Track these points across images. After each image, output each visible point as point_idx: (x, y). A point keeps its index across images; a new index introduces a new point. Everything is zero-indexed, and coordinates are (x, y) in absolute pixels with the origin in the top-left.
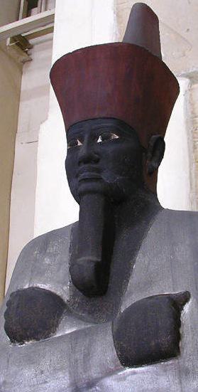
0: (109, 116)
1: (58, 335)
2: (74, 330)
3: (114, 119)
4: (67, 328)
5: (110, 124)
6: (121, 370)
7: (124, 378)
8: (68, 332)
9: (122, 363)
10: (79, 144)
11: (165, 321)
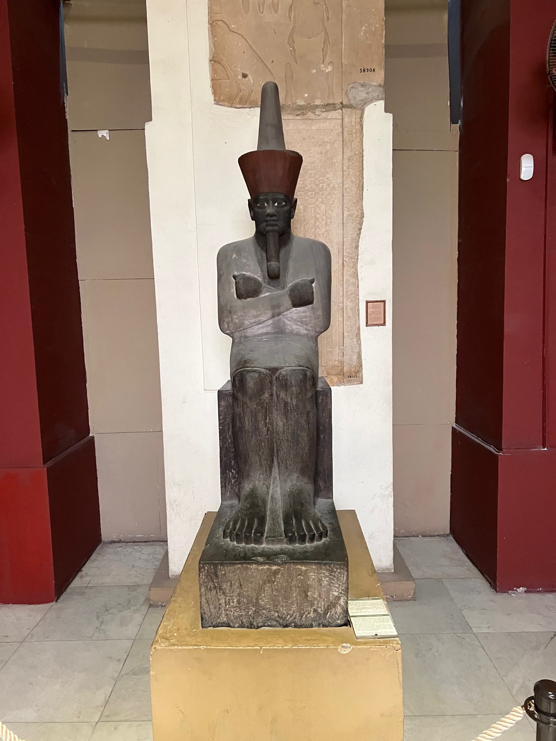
8: (267, 294)
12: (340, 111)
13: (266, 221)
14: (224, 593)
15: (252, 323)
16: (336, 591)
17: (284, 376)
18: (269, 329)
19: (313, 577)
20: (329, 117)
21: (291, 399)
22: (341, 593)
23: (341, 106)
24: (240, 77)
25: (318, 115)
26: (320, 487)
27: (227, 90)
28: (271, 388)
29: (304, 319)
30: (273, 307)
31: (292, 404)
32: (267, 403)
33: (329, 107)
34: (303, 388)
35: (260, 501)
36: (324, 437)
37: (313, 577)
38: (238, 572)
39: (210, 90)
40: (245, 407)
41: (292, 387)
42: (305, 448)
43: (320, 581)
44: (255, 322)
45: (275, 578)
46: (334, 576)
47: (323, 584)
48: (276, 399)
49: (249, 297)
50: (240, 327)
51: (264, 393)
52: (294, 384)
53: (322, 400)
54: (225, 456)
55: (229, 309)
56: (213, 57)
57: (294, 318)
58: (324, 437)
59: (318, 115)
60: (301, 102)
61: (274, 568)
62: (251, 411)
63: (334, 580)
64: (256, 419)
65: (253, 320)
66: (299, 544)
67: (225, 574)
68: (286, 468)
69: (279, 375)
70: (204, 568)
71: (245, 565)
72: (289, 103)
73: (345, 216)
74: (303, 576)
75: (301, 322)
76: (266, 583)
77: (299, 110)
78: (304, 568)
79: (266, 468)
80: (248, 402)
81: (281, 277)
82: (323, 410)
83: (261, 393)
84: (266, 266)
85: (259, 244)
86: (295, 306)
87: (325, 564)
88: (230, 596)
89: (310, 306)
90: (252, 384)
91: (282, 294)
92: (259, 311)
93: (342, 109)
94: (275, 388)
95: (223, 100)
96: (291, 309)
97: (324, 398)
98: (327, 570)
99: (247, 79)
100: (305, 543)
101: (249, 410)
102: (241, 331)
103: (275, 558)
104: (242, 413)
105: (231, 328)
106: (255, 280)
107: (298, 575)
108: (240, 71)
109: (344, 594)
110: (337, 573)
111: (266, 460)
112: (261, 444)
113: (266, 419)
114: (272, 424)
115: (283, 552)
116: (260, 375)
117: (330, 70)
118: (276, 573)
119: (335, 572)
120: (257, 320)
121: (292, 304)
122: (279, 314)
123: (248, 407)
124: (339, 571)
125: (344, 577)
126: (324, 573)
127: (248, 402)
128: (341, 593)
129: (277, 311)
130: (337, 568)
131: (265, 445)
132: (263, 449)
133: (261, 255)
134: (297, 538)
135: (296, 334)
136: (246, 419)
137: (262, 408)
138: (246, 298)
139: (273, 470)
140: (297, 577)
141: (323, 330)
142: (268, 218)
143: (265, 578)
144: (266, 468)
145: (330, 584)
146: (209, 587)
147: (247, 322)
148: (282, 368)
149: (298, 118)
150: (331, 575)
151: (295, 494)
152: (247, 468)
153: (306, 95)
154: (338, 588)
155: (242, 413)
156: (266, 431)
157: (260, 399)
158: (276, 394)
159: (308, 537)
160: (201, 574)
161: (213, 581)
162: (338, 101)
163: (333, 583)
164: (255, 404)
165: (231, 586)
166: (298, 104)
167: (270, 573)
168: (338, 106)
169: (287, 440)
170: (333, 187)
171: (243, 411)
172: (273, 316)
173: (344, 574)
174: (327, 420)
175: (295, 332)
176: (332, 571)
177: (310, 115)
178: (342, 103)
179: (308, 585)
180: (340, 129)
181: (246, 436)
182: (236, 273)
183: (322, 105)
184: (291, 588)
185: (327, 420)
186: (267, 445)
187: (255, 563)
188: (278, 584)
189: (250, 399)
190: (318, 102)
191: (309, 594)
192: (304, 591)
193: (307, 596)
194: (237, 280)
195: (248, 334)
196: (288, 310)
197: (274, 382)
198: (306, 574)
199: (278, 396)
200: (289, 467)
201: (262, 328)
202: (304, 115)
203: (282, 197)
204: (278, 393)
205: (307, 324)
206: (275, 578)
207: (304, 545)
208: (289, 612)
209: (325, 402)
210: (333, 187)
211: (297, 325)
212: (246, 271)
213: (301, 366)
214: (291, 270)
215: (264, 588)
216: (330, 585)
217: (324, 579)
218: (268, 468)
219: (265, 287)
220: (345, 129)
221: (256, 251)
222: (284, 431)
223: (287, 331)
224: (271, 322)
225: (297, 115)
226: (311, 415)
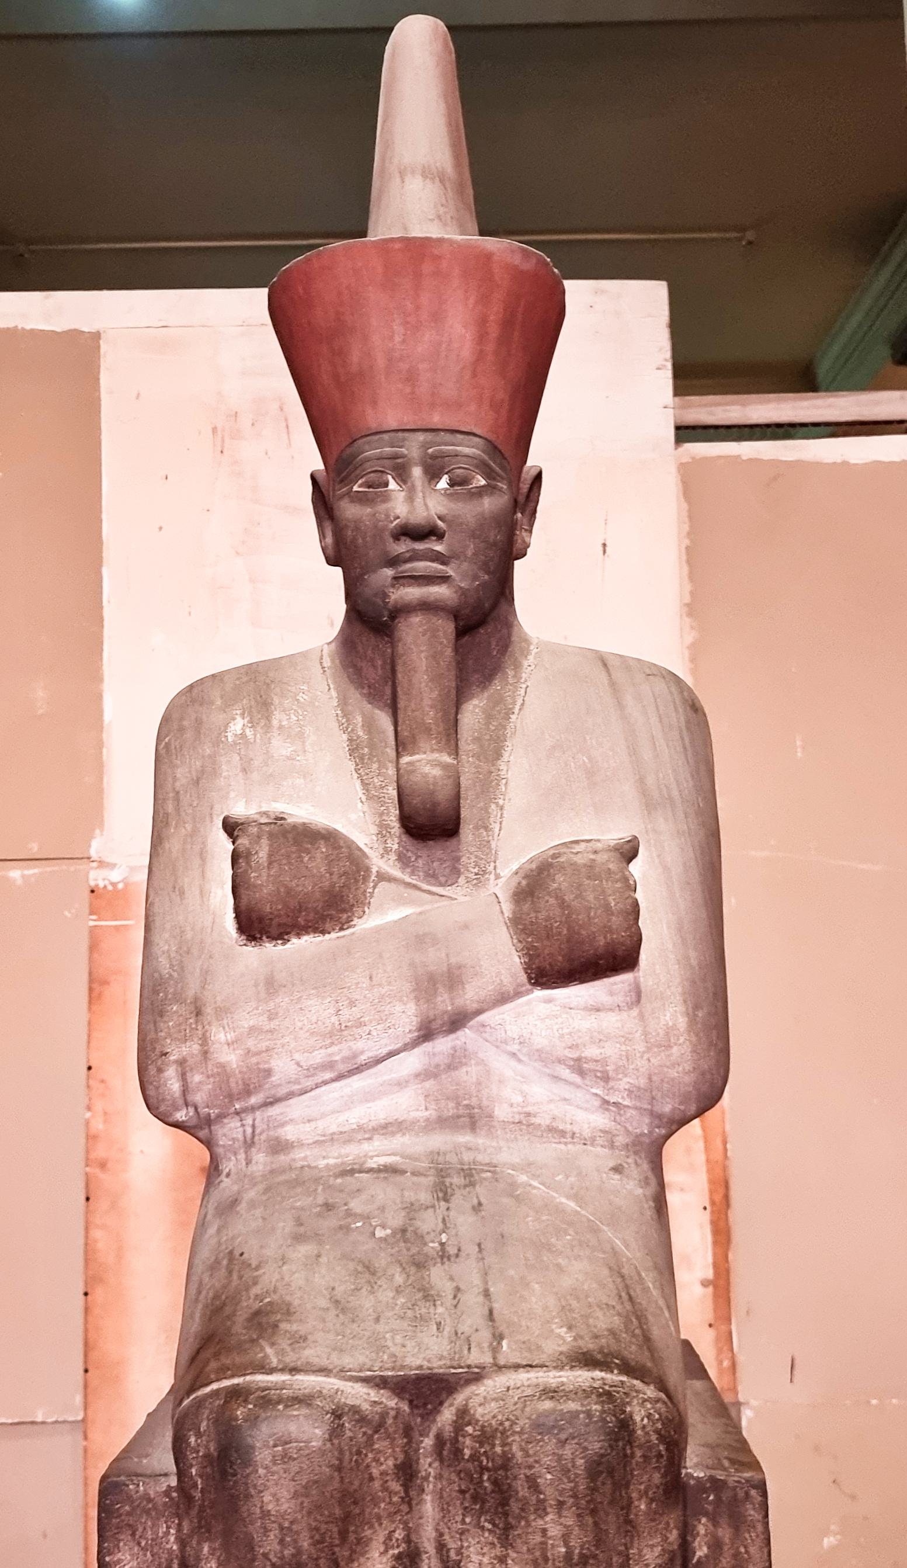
8: (396, 914)
9: (530, 979)
15: (311, 1071)
17: (485, 1436)
18: (408, 1104)
28: (409, 1501)
30: (427, 985)
41: (541, 1509)
44: (329, 1065)
49: (302, 930)
50: (248, 1092)
52: (550, 1494)
55: (190, 994)
57: (540, 1042)
65: (319, 1057)
81: (467, 832)
84: (391, 771)
90: (285, 1494)
91: (475, 918)
92: (352, 1004)
94: (429, 1507)
102: (253, 1109)
105: (199, 1098)
116: (335, 1432)
120: (339, 1052)
121: (527, 968)
122: (457, 1022)
129: (445, 1003)
133: (370, 725)
135: (551, 1129)
138: (281, 935)
141: (693, 1109)
148: (476, 1376)
158: (441, 1547)
172: (426, 1033)
175: (543, 1120)
182: (240, 809)
194: (243, 841)
195: (289, 1133)
196: (503, 998)
197: (427, 1465)
203: (469, 449)
219: (382, 877)
221: (343, 702)
223: (501, 1112)
224: (413, 1061)
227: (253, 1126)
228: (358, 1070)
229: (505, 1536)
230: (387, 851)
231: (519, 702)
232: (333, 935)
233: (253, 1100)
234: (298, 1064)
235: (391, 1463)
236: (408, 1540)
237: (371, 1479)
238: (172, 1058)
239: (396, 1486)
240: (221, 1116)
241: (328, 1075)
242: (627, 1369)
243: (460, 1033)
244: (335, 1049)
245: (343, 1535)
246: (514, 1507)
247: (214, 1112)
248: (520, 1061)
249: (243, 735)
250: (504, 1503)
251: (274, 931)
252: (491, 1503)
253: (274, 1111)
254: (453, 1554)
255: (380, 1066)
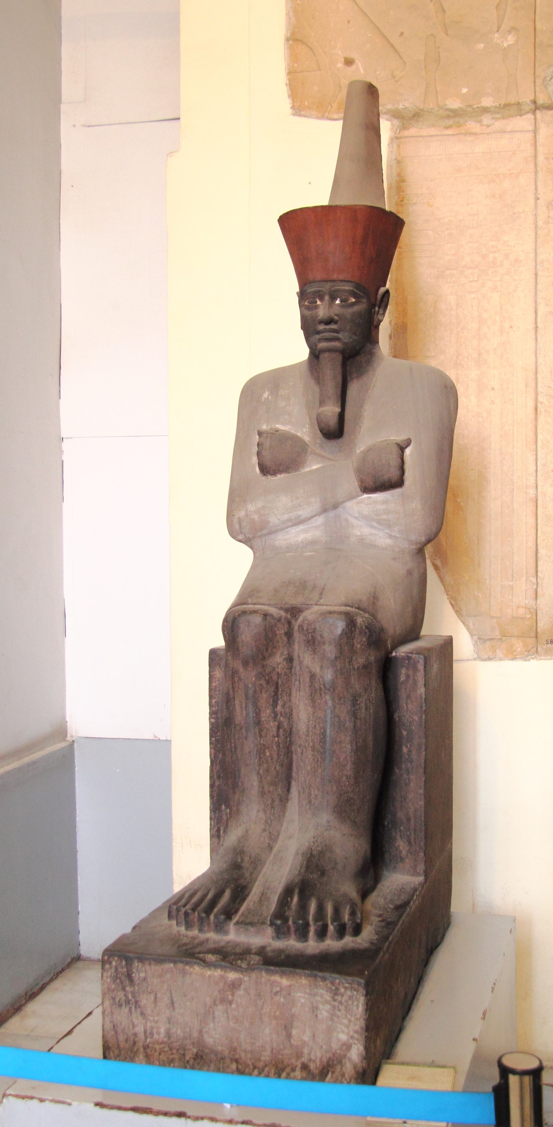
0: (347, 279)
1: (307, 469)
2: (319, 466)
3: (351, 282)
4: (313, 466)
5: (348, 287)
6: (361, 496)
7: (362, 502)
8: (314, 467)
9: (361, 490)
10: (319, 303)
11: (394, 462)
12: (530, 116)
13: (318, 333)
14: (142, 1014)
16: (343, 1032)
19: (303, 1000)
20: (509, 129)
21: (321, 667)
22: (352, 1037)
23: (532, 107)
24: (340, 65)
25: (488, 126)
26: (401, 852)
27: (316, 88)
29: (384, 517)
31: (322, 677)
32: (278, 674)
33: (509, 109)
34: (346, 649)
35: (246, 859)
36: (410, 751)
37: (303, 1000)
38: (168, 976)
39: (283, 91)
40: (236, 679)
41: (324, 643)
42: (345, 766)
43: (314, 1009)
44: (290, 520)
45: (233, 995)
46: (341, 1003)
47: (320, 1017)
48: (298, 668)
50: (262, 529)
51: (272, 655)
53: (408, 676)
54: (219, 777)
56: (293, 33)
58: (410, 751)
59: (488, 126)
60: (454, 104)
61: (232, 976)
62: (246, 687)
63: (339, 1010)
64: (255, 704)
65: (286, 517)
66: (294, 940)
67: (145, 979)
68: (310, 802)
69: (303, 621)
70: (110, 963)
71: (180, 966)
72: (431, 106)
73: (539, 314)
74: (285, 997)
75: (379, 522)
76: (218, 1002)
77: (448, 117)
78: (285, 982)
79: (273, 801)
80: (241, 669)
82: (409, 697)
83: (266, 654)
85: (312, 373)
86: (367, 489)
87: (324, 979)
88: (154, 1021)
89: (397, 491)
92: (297, 498)
93: (534, 112)
95: (309, 108)
96: (358, 496)
97: (411, 672)
98: (329, 990)
99: (353, 67)
100: (306, 940)
101: (242, 686)
103: (239, 959)
104: (231, 692)
105: (245, 531)
106: (295, 439)
107: (276, 993)
108: (340, 55)
109: (357, 1040)
110: (345, 998)
111: (274, 784)
112: (264, 752)
113: (275, 704)
114: (289, 716)
115: (261, 951)
117: (511, 43)
118: (234, 986)
119: (342, 996)
122: (335, 507)
123: (240, 679)
124: (349, 993)
125: (358, 1007)
126: (322, 996)
127: (241, 669)
128: (352, 1037)
130: (346, 988)
131: (271, 756)
132: (267, 762)
134: (292, 929)
136: (237, 702)
137: (268, 682)
138: (274, 473)
139: (289, 805)
140: (272, 998)
142: (321, 327)
143: (216, 993)
144: (273, 801)
145: (332, 1017)
146: (117, 1000)
147: (274, 520)
148: (308, 606)
149: (449, 132)
150: (335, 1000)
151: (315, 853)
152: (236, 797)
153: (465, 91)
154: (347, 1027)
155: (231, 692)
156: (275, 730)
157: (263, 666)
159: (312, 929)
160: (105, 974)
161: (124, 989)
162: (527, 98)
163: (338, 1017)
164: (254, 673)
165: (155, 1001)
166: (449, 106)
167: (225, 983)
168: (527, 108)
169: (313, 749)
170: (517, 260)
171: (233, 688)
172: (324, 510)
173: (358, 1000)
174: (416, 718)
176: (336, 993)
177: (472, 125)
178: (534, 102)
179: (293, 1015)
180: (530, 151)
181: (237, 736)
182: (264, 427)
183: (496, 107)
184: (261, 1018)
185: (416, 718)
186: (275, 756)
187: (198, 964)
188: (238, 1005)
189: (245, 664)
190: (487, 102)
191: (294, 1032)
192: (286, 1027)
193: (289, 1036)
196: (351, 498)
197: (296, 635)
198: (289, 994)
199: (301, 662)
200: (313, 801)
201: (306, 531)
202: (459, 127)
204: (301, 656)
205: (389, 527)
206: (233, 995)
207: (305, 944)
208: (257, 1064)
209: (411, 681)
210: (517, 260)
211: (372, 527)
212: (283, 424)
213: (347, 605)
214: (367, 422)
215: (214, 1013)
216: (332, 1019)
217: (321, 1006)
218: (277, 802)
220: (540, 149)
222: (308, 731)
224: (320, 520)
225: (447, 128)
226: (362, 701)
227: (265, 542)
228: (299, 522)
229: (314, 651)
230: (316, 443)
231: (373, 385)
232: (292, 474)
233: (264, 532)
234: (279, 519)
235: (283, 631)
236: (289, 654)
237: (276, 635)
238: (236, 516)
239: (285, 639)
240: (254, 537)
241: (290, 524)
242: (358, 608)
243: (337, 510)
244: (291, 514)
245: (267, 650)
246: (317, 642)
247: (251, 536)
248: (359, 520)
249: (268, 398)
250: (314, 642)
251: (271, 472)
252: (311, 643)
253: (272, 536)
254: (302, 659)
255: (310, 521)
